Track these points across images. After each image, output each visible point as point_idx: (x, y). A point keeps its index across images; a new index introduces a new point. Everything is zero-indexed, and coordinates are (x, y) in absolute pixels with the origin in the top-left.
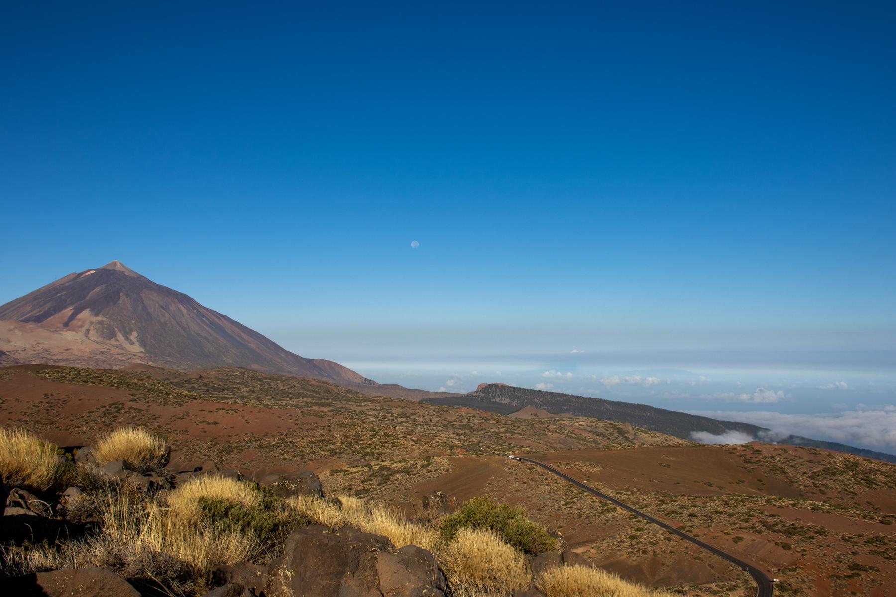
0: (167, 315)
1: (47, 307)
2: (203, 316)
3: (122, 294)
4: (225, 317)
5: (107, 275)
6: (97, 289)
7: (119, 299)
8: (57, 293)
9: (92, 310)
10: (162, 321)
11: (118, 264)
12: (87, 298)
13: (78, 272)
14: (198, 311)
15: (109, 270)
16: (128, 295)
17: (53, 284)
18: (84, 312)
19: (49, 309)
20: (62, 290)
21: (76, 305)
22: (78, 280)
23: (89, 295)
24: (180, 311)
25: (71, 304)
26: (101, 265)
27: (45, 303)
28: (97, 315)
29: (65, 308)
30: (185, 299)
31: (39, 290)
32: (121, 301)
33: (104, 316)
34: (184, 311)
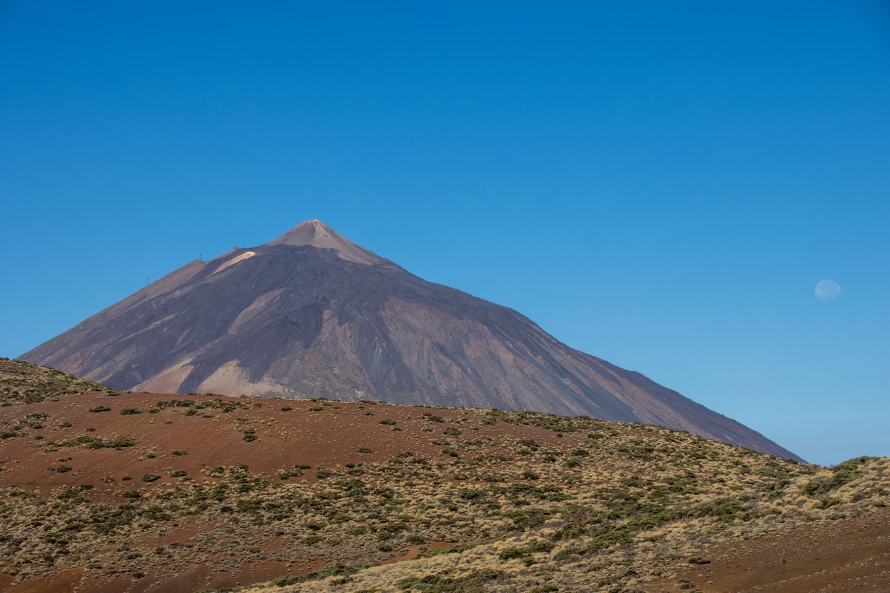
0: (456, 370)
1: (122, 359)
2: (564, 372)
3: (326, 314)
4: (636, 378)
5: (287, 263)
6: (259, 304)
7: (318, 329)
9: (242, 365)
10: (443, 389)
11: (320, 231)
12: (232, 331)
13: (208, 258)
14: (547, 356)
15: (295, 249)
16: (343, 318)
17: (142, 294)
18: (221, 371)
19: (128, 367)
20: (165, 310)
21: (202, 350)
22: (209, 280)
23: (239, 321)
24: (495, 359)
26: (271, 236)
27: (117, 351)
28: (255, 378)
29: (171, 360)
30: (510, 325)
31: (104, 314)
32: (325, 336)
33: (277, 379)
34: (508, 358)
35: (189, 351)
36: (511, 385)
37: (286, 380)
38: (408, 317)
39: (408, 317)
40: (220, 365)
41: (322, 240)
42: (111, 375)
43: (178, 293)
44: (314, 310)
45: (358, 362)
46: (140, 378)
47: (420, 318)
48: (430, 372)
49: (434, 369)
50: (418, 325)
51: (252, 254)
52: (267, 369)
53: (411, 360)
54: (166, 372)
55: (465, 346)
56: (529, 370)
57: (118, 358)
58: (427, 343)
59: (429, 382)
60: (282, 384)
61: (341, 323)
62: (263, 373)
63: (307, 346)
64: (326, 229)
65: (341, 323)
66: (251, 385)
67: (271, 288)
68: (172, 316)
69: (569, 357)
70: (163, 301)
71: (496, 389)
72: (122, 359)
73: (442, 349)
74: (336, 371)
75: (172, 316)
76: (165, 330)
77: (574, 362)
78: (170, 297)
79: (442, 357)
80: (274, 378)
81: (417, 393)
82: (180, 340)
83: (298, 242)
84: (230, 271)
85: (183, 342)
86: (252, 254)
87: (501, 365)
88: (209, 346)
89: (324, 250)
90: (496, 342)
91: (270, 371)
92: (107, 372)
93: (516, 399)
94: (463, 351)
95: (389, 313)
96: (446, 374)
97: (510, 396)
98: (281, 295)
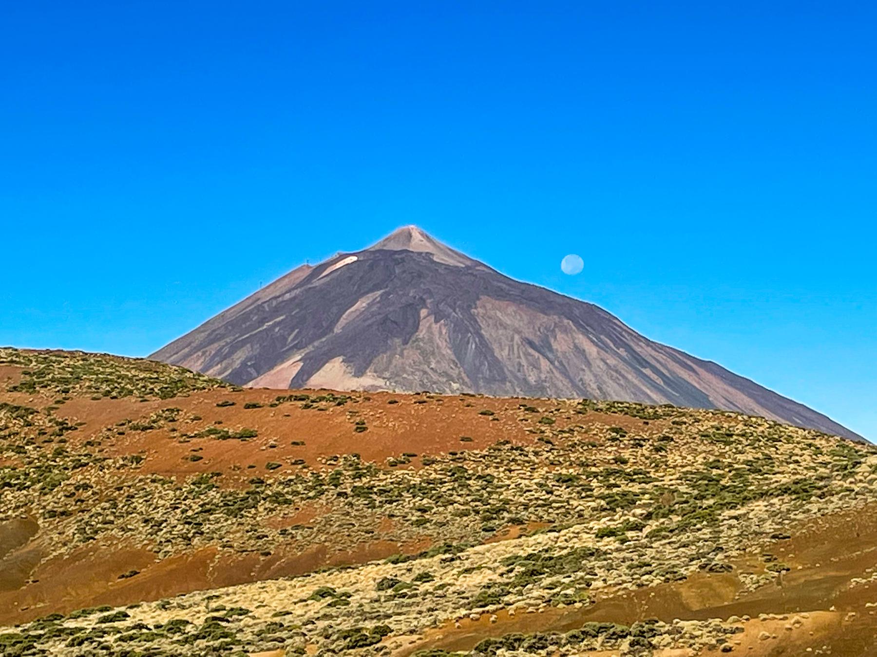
0: (544, 364)
1: (239, 357)
2: (645, 364)
3: (423, 312)
6: (361, 304)
7: (416, 327)
8: (262, 322)
10: (532, 379)
12: (337, 330)
13: (314, 265)
16: (438, 316)
19: (244, 364)
20: (276, 311)
21: (310, 348)
22: (316, 283)
23: (343, 321)
24: (580, 352)
25: (297, 347)
29: (282, 357)
30: (594, 321)
32: (422, 333)
33: (379, 373)
34: (592, 350)
35: (299, 349)
36: (595, 376)
37: (387, 375)
38: (499, 314)
39: (499, 314)
40: (327, 362)
41: (418, 243)
42: (230, 371)
43: (288, 296)
44: (412, 308)
45: (453, 357)
46: (255, 374)
47: (511, 316)
48: (520, 364)
49: (524, 362)
50: (509, 322)
51: (355, 258)
52: (368, 365)
53: (502, 354)
54: (278, 368)
55: (552, 340)
56: (612, 361)
57: (235, 356)
58: (517, 337)
59: (519, 374)
60: (384, 378)
61: (436, 322)
62: (366, 368)
63: (405, 342)
64: (422, 235)
65: (436, 322)
66: (356, 379)
67: (372, 290)
68: (282, 318)
69: (649, 349)
70: (274, 303)
71: (581, 380)
72: (239, 357)
73: (531, 344)
74: (433, 366)
75: (282, 318)
76: (277, 329)
77: (654, 353)
78: (280, 299)
79: (531, 351)
80: (375, 372)
81: (508, 384)
82: (290, 339)
83: (398, 248)
84: (335, 274)
85: (293, 340)
86: (355, 258)
87: (586, 358)
88: (316, 344)
89: (420, 254)
90: (581, 336)
91: (372, 367)
92: (225, 369)
93: (600, 389)
94: (550, 346)
95: (481, 311)
96: (536, 366)
97: (594, 386)
98: (381, 296)
